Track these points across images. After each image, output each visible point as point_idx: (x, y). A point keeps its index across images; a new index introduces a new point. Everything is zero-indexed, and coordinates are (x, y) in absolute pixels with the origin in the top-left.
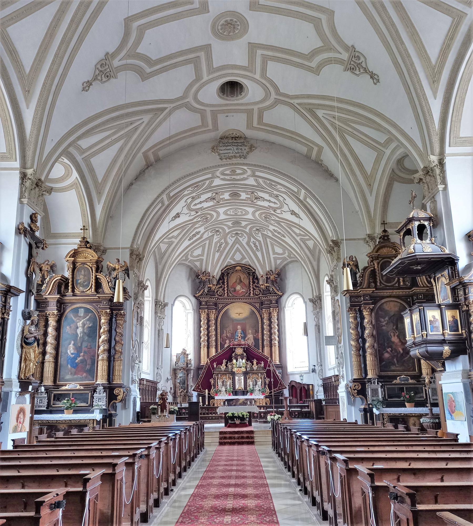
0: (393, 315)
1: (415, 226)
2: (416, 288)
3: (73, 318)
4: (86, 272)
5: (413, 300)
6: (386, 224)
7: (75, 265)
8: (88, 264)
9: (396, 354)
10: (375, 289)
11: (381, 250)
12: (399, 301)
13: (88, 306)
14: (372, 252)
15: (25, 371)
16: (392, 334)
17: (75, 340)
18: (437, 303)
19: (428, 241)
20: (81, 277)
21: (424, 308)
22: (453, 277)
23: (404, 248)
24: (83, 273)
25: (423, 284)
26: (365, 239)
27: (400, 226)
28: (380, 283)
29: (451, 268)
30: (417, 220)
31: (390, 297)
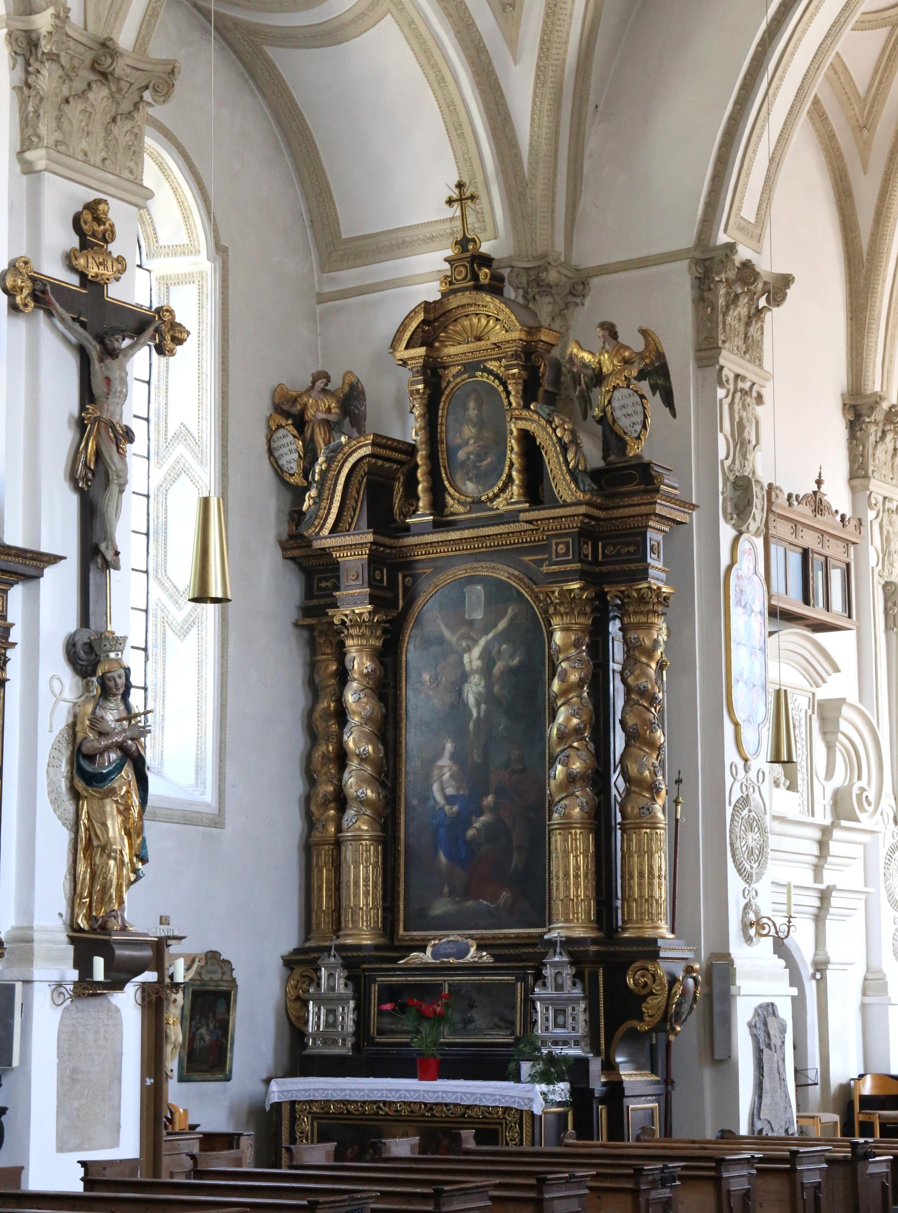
3: (447, 634)
4: (484, 407)
7: (440, 378)
8: (492, 365)
13: (503, 573)
15: (90, 895)
17: (459, 735)
20: (469, 431)
24: (472, 413)
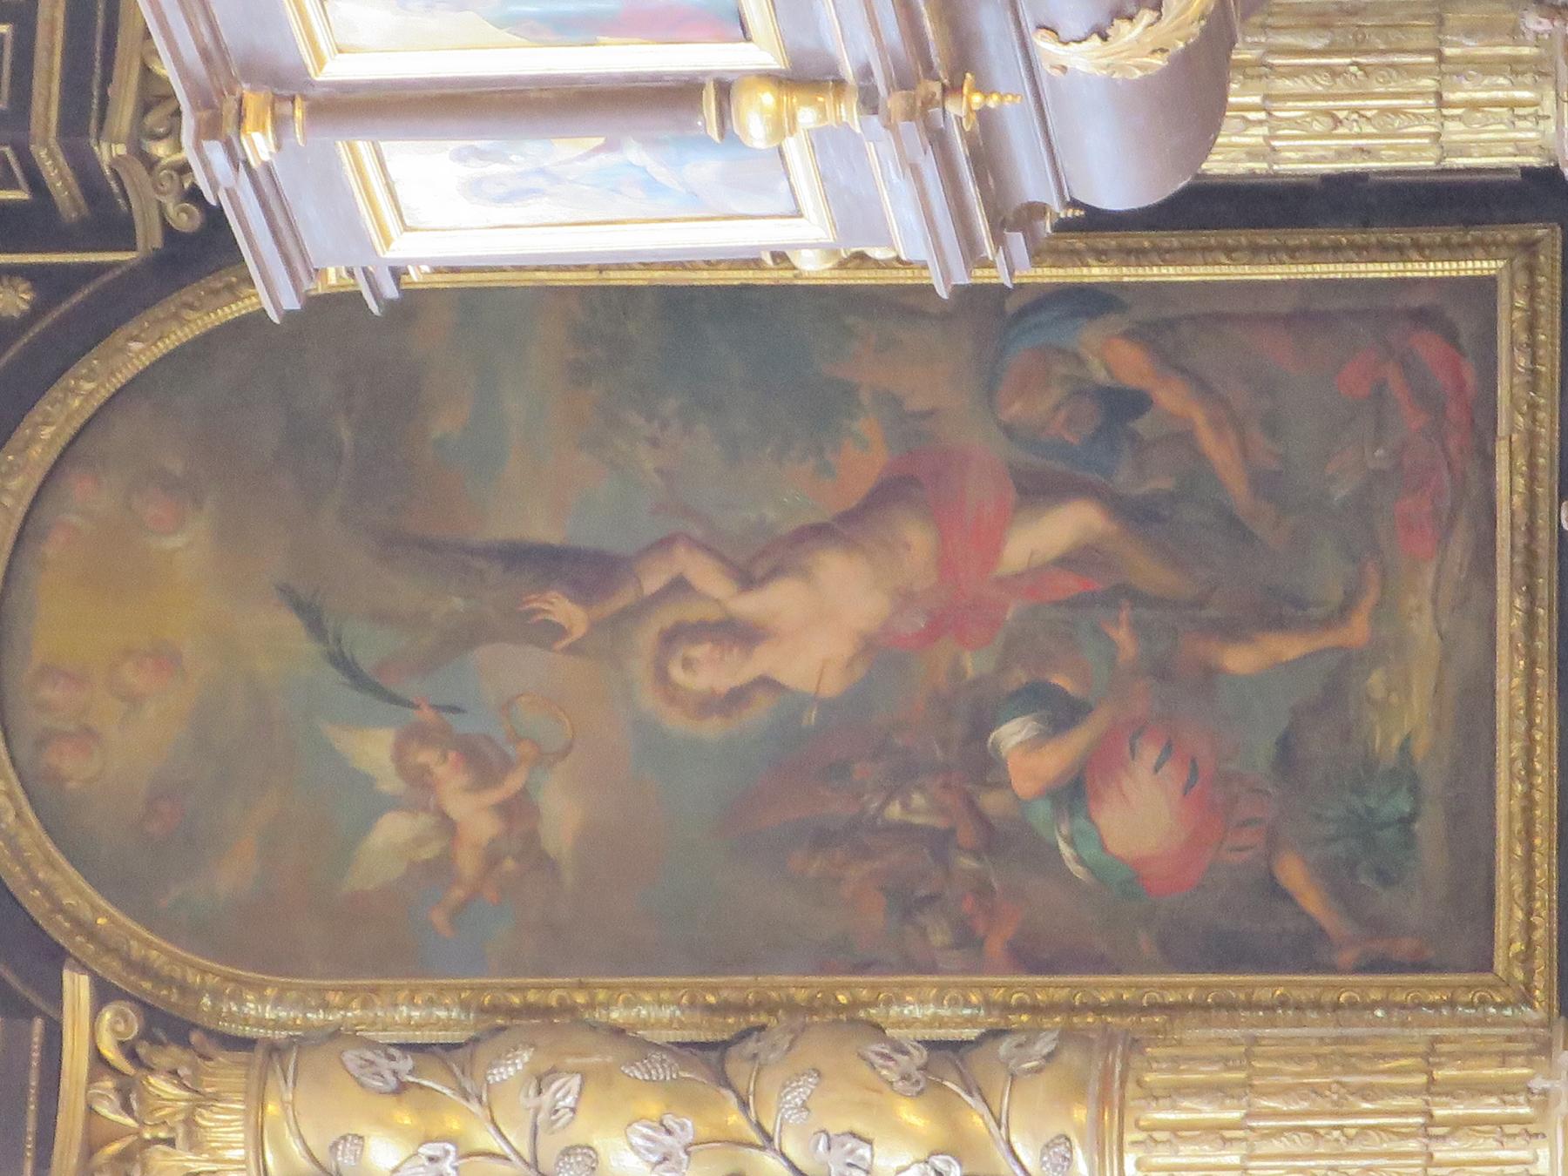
0: (313, 618)
9: (1122, 635)
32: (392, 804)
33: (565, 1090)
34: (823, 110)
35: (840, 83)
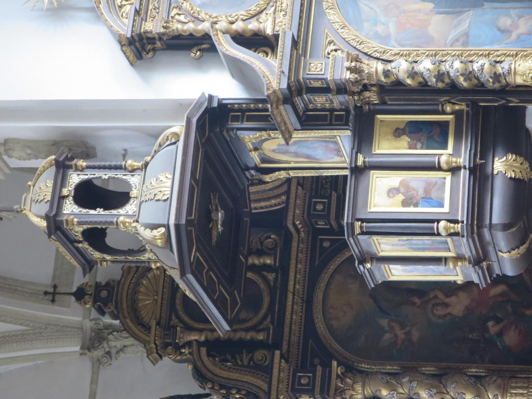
1: (76, 215)
2: (290, 218)
5: (330, 231)
6: (55, 287)
9: (509, 308)
10: (277, 353)
11: (143, 313)
12: (325, 277)
14: (145, 343)
16: (440, 311)
18: (346, 172)
19: (134, 180)
21: (358, 220)
22: (266, 119)
23: (147, 256)
25: (279, 196)
26: (98, 364)
27: (68, 257)
28: (258, 331)
29: (236, 119)
30: (60, 207)
31: (309, 303)
32: (387, 332)
33: (414, 384)
34: (462, 263)
35: (465, 258)
